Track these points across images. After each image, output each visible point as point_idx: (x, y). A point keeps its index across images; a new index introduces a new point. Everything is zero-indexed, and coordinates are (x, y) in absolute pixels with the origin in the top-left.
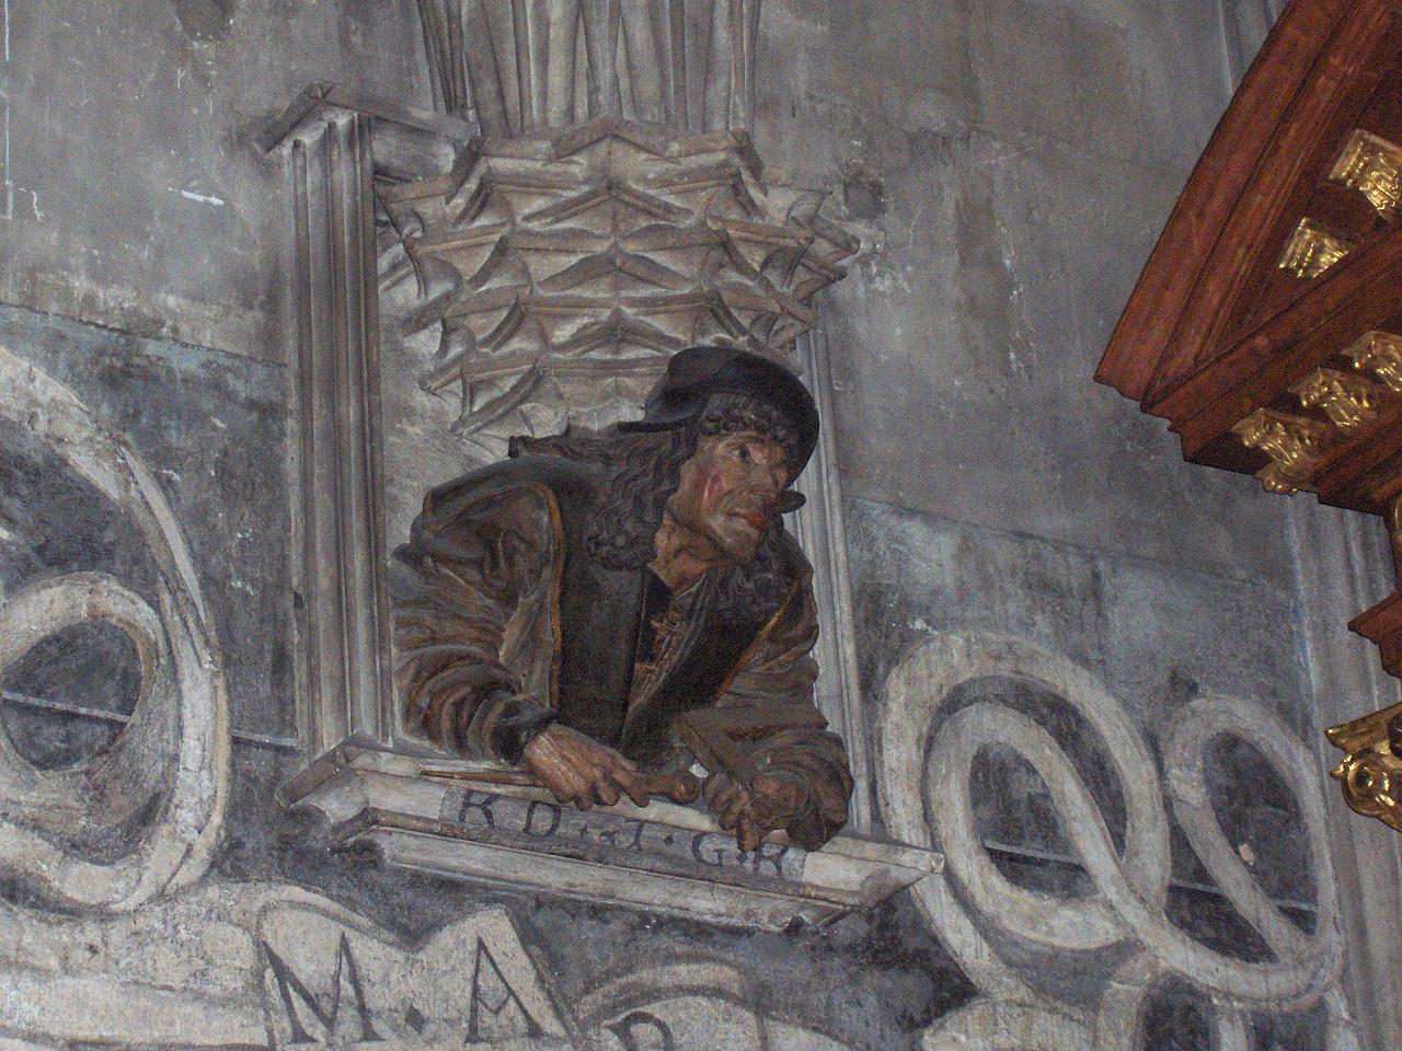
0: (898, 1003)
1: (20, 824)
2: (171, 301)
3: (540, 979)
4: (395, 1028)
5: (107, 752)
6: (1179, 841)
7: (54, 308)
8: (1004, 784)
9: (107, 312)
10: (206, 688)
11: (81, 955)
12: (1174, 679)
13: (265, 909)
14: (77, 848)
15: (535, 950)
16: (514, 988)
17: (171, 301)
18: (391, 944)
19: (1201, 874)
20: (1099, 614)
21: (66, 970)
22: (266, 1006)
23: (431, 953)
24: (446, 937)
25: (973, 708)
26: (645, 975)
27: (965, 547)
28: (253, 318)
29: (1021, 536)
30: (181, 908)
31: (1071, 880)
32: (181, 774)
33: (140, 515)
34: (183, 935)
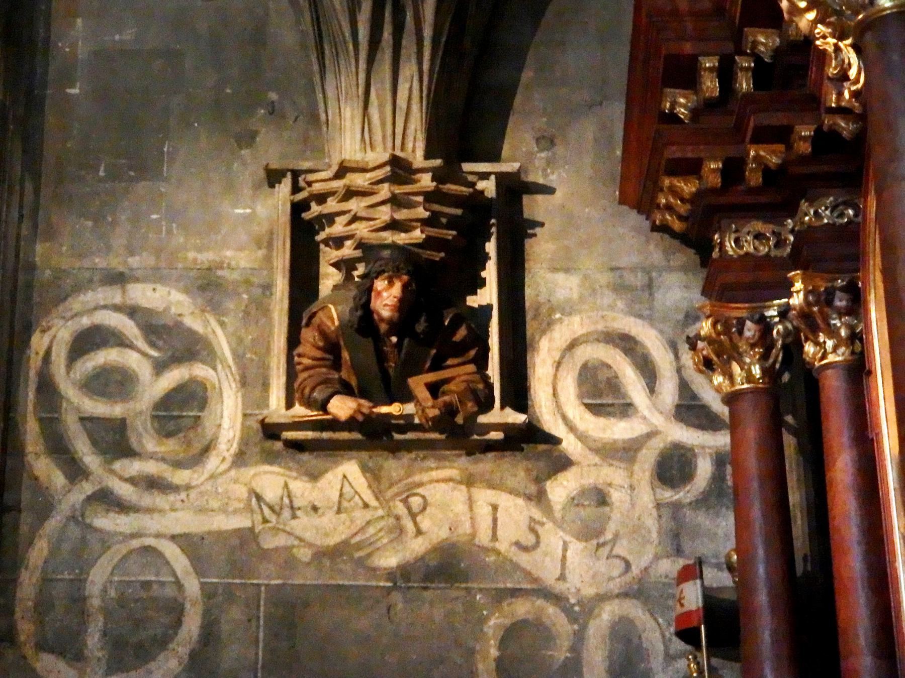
0: (535, 473)
1: (157, 460)
2: (229, 253)
3: (370, 486)
4: (307, 513)
5: (193, 428)
6: (684, 387)
7: (180, 266)
8: (595, 376)
9: (201, 263)
10: (233, 397)
11: (179, 505)
12: (687, 316)
13: (255, 475)
14: (178, 464)
15: (368, 475)
16: (358, 490)
17: (229, 253)
18: (306, 482)
19: (694, 397)
20: (651, 294)
21: (173, 510)
22: (252, 512)
23: (323, 482)
24: (329, 476)
25: (582, 346)
26: (417, 478)
27: (586, 277)
28: (261, 253)
29: (613, 269)
30: (220, 480)
31: (626, 409)
32: (222, 431)
33: (211, 336)
34: (220, 490)
